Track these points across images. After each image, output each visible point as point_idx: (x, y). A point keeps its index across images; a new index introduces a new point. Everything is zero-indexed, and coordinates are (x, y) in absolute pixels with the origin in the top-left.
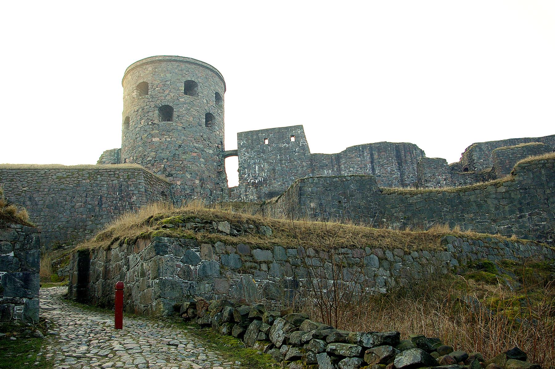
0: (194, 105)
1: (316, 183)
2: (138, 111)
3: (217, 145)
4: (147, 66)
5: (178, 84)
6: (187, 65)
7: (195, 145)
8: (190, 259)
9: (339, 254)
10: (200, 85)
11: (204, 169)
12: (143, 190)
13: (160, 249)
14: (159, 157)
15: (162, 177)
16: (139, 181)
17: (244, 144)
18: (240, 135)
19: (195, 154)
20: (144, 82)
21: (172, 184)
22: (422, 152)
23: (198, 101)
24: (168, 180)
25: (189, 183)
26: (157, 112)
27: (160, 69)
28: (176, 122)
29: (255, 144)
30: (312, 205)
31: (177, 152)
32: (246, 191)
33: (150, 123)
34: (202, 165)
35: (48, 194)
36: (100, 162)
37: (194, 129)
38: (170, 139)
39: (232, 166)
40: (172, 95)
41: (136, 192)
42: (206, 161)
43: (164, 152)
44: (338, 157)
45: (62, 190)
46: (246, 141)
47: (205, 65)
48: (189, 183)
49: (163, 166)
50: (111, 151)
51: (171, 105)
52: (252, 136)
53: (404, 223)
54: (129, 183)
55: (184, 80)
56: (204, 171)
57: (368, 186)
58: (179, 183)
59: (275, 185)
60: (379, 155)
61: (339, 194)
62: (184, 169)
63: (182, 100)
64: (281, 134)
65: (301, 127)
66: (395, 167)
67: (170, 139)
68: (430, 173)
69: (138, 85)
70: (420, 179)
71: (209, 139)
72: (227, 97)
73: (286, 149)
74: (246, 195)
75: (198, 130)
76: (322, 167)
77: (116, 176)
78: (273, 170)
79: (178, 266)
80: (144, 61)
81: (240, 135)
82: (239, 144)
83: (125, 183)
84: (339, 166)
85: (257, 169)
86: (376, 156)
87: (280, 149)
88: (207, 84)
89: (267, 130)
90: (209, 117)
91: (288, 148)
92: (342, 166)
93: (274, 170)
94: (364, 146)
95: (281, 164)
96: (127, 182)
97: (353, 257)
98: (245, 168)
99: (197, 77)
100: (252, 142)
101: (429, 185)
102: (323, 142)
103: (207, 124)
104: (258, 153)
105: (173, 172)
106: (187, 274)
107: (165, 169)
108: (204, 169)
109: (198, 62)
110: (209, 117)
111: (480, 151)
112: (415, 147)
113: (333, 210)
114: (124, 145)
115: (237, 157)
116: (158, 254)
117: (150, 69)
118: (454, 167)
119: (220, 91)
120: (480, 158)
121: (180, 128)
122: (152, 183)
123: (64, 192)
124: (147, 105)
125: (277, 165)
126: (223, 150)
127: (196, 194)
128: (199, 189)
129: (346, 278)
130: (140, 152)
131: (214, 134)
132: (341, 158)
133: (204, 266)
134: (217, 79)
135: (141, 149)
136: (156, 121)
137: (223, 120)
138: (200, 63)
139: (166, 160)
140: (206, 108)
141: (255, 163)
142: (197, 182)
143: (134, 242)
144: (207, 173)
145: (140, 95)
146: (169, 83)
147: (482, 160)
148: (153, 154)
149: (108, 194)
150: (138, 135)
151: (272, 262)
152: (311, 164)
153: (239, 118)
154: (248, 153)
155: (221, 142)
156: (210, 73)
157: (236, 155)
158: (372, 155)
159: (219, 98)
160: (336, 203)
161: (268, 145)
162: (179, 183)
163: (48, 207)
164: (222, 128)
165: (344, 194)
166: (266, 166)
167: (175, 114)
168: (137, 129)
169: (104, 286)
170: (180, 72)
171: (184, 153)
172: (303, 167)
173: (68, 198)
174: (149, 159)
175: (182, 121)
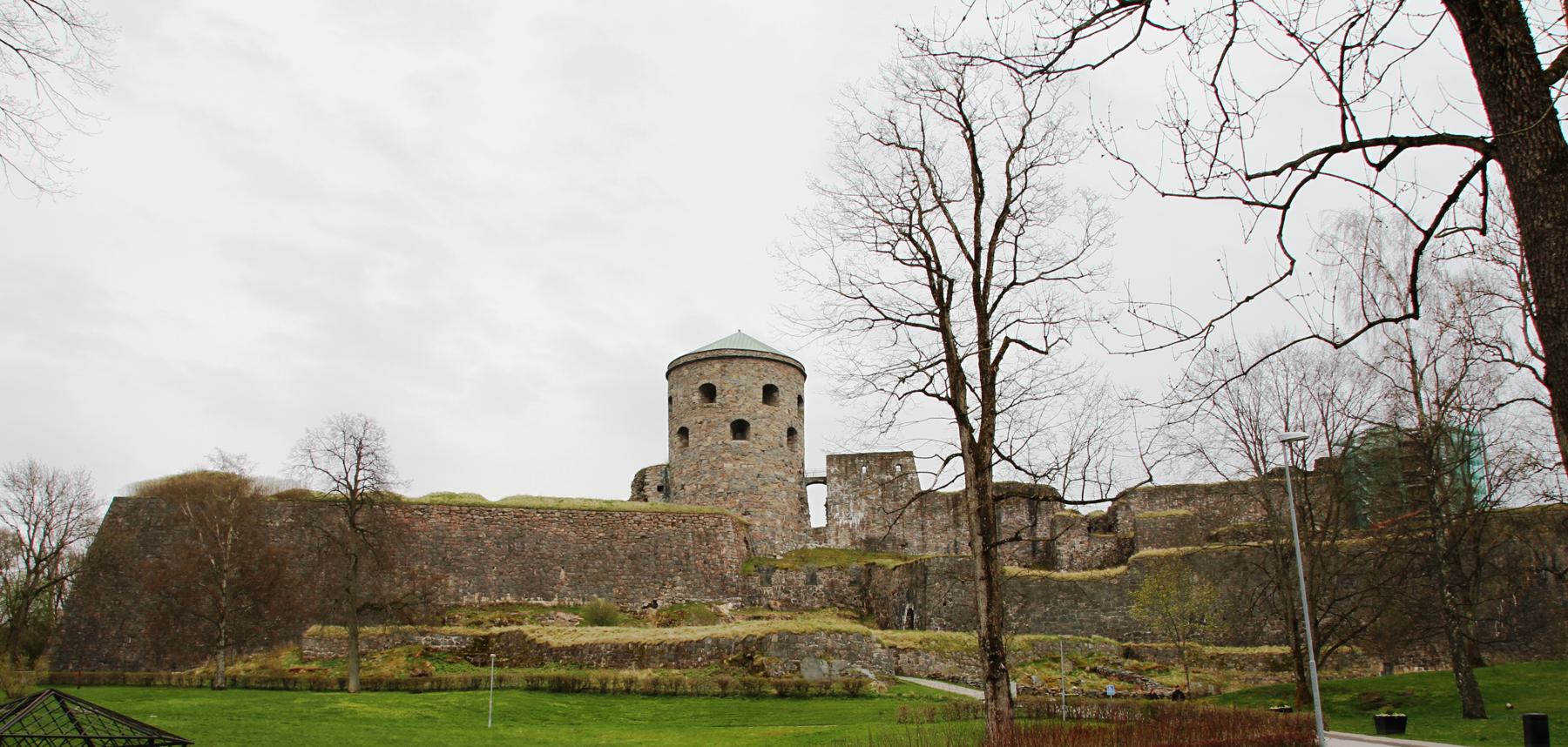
18: (830, 459)
24: (745, 519)
39: (817, 496)
55: (762, 384)
64: (885, 460)
65: (910, 454)
76: (935, 510)
81: (830, 459)
90: (792, 432)
99: (775, 376)
104: (854, 484)
110: (792, 432)
128: (780, 531)
134: (799, 376)
143: (904, 650)
148: (725, 485)
167: (752, 431)
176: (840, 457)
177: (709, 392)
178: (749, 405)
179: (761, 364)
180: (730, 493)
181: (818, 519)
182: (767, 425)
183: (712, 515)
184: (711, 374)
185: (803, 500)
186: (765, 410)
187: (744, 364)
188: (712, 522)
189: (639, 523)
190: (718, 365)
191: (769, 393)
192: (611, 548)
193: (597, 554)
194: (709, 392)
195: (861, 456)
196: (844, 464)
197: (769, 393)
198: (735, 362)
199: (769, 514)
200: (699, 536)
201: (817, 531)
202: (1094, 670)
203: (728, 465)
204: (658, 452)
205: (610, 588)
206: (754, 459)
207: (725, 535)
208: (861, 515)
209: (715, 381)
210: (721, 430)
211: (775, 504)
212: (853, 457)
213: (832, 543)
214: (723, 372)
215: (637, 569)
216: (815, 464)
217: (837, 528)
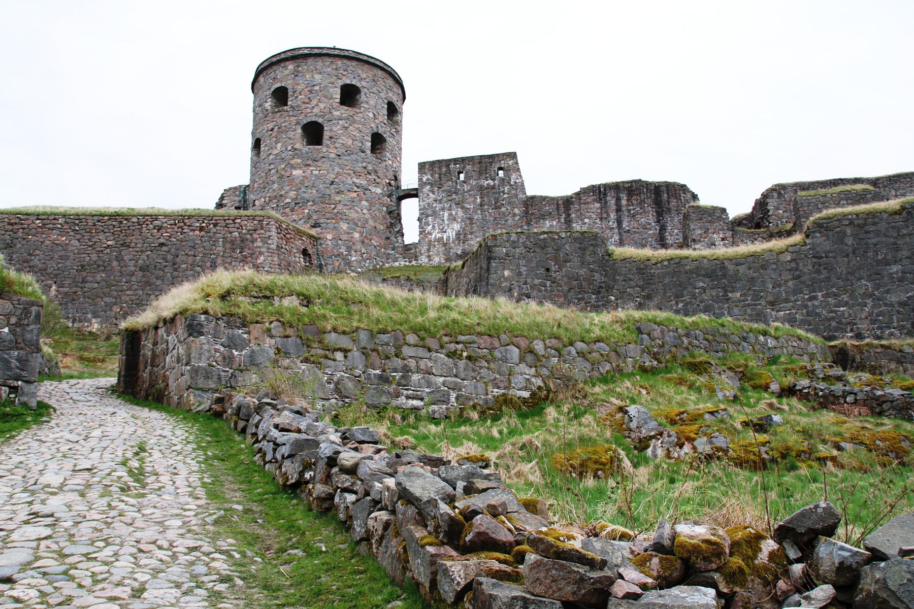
0: (354, 122)
1: (514, 242)
2: (272, 130)
3: (388, 181)
4: (287, 63)
5: (331, 90)
6: (345, 61)
7: (355, 180)
8: (232, 344)
9: (457, 343)
10: (363, 91)
11: (368, 216)
12: (274, 246)
13: (194, 329)
14: (303, 198)
15: (305, 228)
16: (268, 234)
17: (428, 179)
18: (422, 166)
19: (355, 195)
20: (281, 87)
21: (320, 238)
22: (695, 197)
23: (360, 115)
24: (313, 232)
25: (344, 237)
26: (299, 131)
27: (305, 67)
28: (328, 146)
29: (444, 180)
30: (506, 273)
31: (328, 192)
32: (429, 250)
33: (289, 148)
34: (365, 211)
35: (142, 251)
36: (220, 205)
37: (354, 157)
38: (317, 172)
39: (410, 209)
40: (322, 106)
41: (264, 250)
42: (371, 204)
43: (310, 191)
44: (567, 202)
45: (162, 244)
46: (432, 175)
47: (372, 61)
48: (344, 237)
49: (306, 211)
50: (235, 188)
51: (320, 120)
52: (440, 168)
53: (640, 304)
54: (255, 236)
55: (340, 83)
56: (367, 220)
57: (591, 248)
58: (329, 237)
59: (472, 242)
60: (628, 200)
61: (547, 259)
62: (339, 217)
63: (338, 113)
65: (513, 156)
66: (651, 218)
67: (317, 172)
68: (700, 228)
69: (274, 92)
70: (685, 238)
71: (376, 172)
72: (408, 111)
73: (489, 187)
74: (429, 256)
75: (360, 160)
76: (543, 217)
77: (237, 225)
78: (469, 219)
79: (216, 350)
80: (283, 56)
81: (422, 166)
82: (420, 180)
83: (249, 236)
84: (569, 215)
85: (446, 218)
86: (624, 202)
87: (481, 188)
88: (374, 90)
89: (463, 160)
90: (378, 141)
91: (493, 187)
92: (573, 215)
93: (471, 219)
94: (606, 186)
95: (483, 211)
96: (251, 235)
97: (479, 348)
98: (427, 216)
100: (440, 178)
101: (697, 246)
102: (547, 176)
103: (373, 150)
104: (449, 193)
105: (322, 221)
106: (228, 360)
107: (310, 217)
108: (368, 216)
109: (361, 57)
110: (378, 141)
111: (779, 197)
112: (684, 188)
113: (536, 281)
114: (253, 181)
115: (417, 199)
116: (190, 335)
117: (291, 67)
118: (739, 222)
119: (395, 99)
120: (777, 209)
121: (332, 156)
122: (288, 236)
123: (164, 248)
124: (285, 122)
125: (476, 213)
126: (398, 187)
127: (353, 253)
128: (359, 246)
129: (462, 375)
130: (274, 190)
131: (384, 164)
132: (572, 203)
133: (253, 352)
134: (390, 82)
135: (275, 186)
136: (298, 146)
137: (399, 143)
138: (365, 58)
139: (310, 203)
140: (373, 125)
141: (443, 209)
142: (357, 235)
144: (371, 222)
145: (276, 106)
146: (317, 88)
147: (781, 212)
148: (292, 194)
149: (224, 252)
150: (272, 166)
151: (349, 351)
152: (526, 212)
153: (424, 138)
154: (433, 193)
155: (395, 177)
156: (380, 72)
157: (416, 196)
158: (618, 199)
159: (393, 111)
160: (542, 270)
161: (464, 182)
162: (329, 237)
163: (141, 269)
164: (397, 156)
165: (556, 259)
166: (460, 213)
167: (326, 134)
168: (271, 157)
169: (150, 373)
170: (334, 72)
171: (338, 193)
172: (515, 215)
173: (169, 257)
174: (288, 200)
175: (337, 145)
176: (433, 164)
177: (281, 96)
178: (323, 104)
179: (339, 63)
180: (298, 203)
181: (411, 234)
182: (347, 131)
183: (254, 218)
184: (283, 76)
185: (395, 216)
186: (345, 111)
187: (319, 63)
188: (250, 225)
189: (159, 228)
190: (291, 66)
191: (349, 95)
192: (119, 259)
193: (103, 267)
194: (281, 96)
195: (455, 161)
196: (439, 171)
197: (349, 95)
198: (310, 61)
199: (344, 226)
200: (232, 242)
201: (407, 248)
202: (789, 391)
203: (297, 173)
204: (242, 176)
205: (109, 306)
206: (326, 165)
207: (265, 241)
208: (457, 226)
209: (288, 84)
210: (291, 134)
211: (354, 215)
212: (447, 162)
213: (423, 260)
214: (296, 74)
215: (148, 283)
216: (409, 179)
217: (430, 243)
